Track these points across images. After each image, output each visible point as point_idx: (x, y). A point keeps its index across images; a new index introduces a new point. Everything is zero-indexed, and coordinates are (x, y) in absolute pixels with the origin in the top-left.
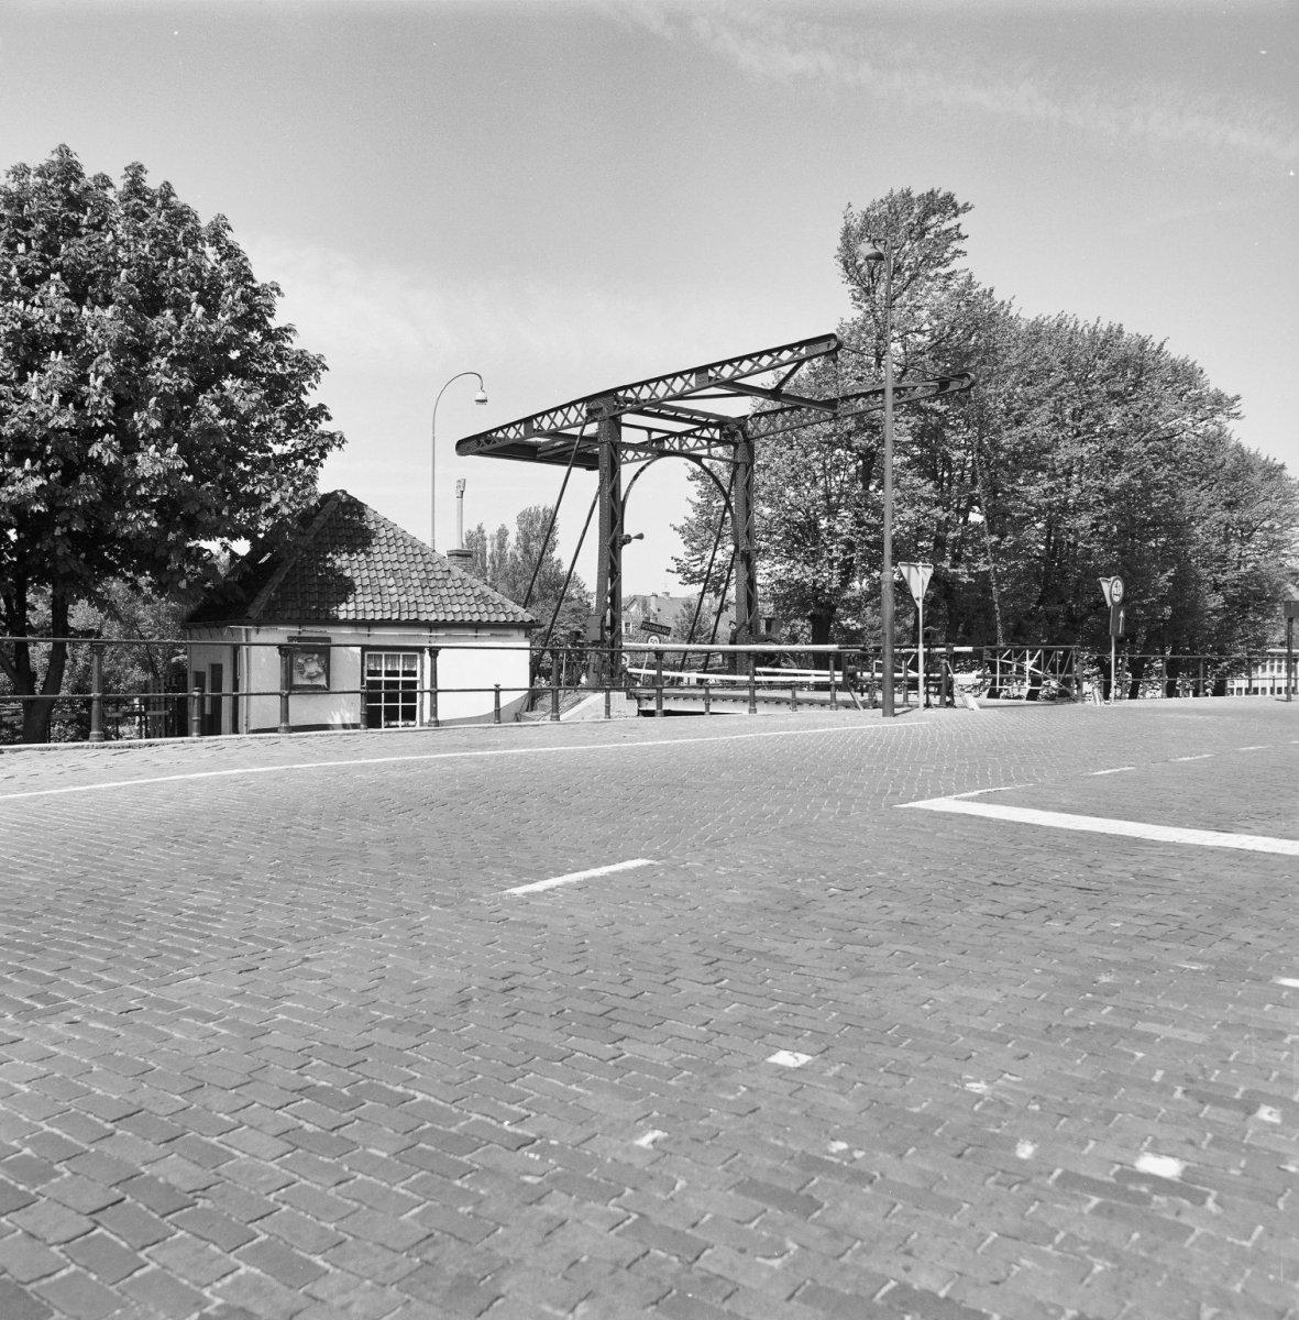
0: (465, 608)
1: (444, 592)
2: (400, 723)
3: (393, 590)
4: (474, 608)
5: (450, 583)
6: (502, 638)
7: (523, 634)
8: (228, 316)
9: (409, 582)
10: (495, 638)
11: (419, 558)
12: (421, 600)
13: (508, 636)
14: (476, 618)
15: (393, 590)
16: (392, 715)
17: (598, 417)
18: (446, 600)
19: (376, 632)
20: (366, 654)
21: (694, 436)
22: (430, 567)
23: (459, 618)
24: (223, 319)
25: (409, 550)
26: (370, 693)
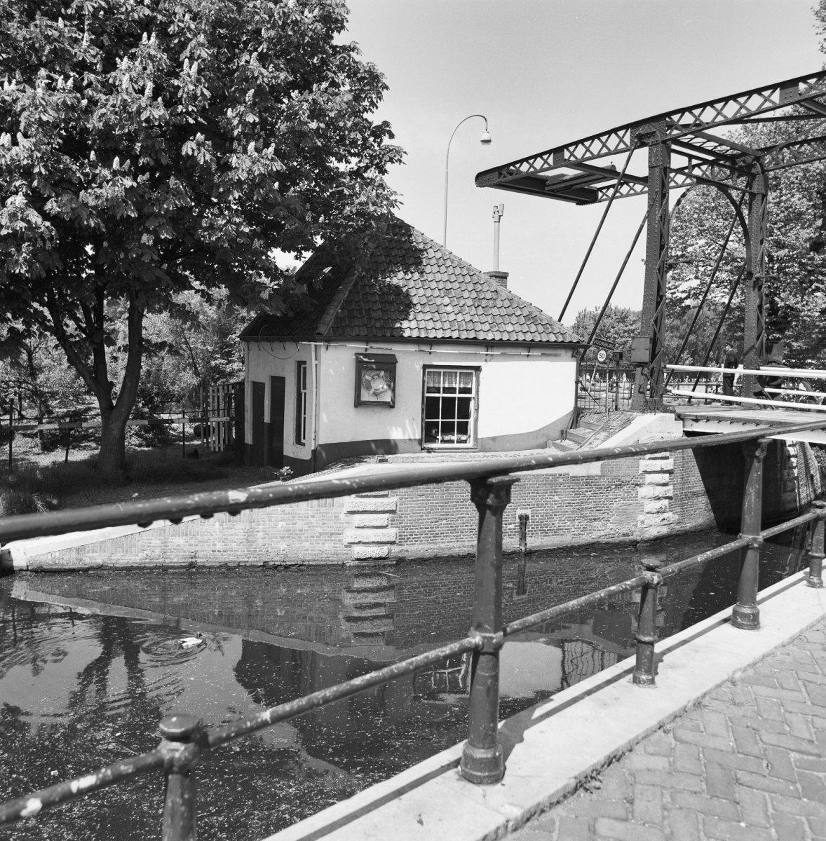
0: (517, 328)
1: (495, 311)
2: (455, 438)
3: (449, 309)
4: (525, 329)
5: (499, 303)
6: (551, 358)
7: (570, 354)
8: (316, 12)
9: (462, 302)
10: (544, 358)
11: (468, 279)
12: (476, 319)
13: (556, 355)
14: (529, 337)
15: (449, 309)
16: (448, 429)
17: (650, 141)
18: (499, 320)
19: (439, 350)
20: (427, 370)
21: (684, 174)
22: (479, 287)
23: (513, 338)
24: (310, 15)
25: (458, 271)
26: (430, 407)
